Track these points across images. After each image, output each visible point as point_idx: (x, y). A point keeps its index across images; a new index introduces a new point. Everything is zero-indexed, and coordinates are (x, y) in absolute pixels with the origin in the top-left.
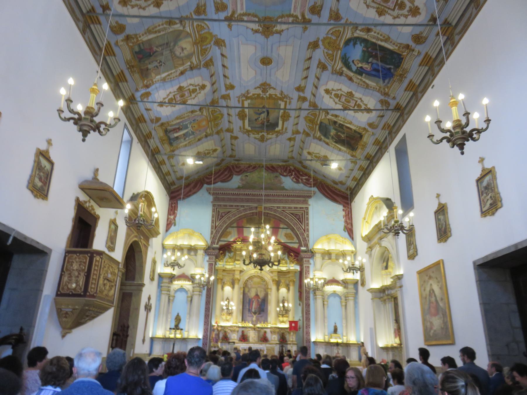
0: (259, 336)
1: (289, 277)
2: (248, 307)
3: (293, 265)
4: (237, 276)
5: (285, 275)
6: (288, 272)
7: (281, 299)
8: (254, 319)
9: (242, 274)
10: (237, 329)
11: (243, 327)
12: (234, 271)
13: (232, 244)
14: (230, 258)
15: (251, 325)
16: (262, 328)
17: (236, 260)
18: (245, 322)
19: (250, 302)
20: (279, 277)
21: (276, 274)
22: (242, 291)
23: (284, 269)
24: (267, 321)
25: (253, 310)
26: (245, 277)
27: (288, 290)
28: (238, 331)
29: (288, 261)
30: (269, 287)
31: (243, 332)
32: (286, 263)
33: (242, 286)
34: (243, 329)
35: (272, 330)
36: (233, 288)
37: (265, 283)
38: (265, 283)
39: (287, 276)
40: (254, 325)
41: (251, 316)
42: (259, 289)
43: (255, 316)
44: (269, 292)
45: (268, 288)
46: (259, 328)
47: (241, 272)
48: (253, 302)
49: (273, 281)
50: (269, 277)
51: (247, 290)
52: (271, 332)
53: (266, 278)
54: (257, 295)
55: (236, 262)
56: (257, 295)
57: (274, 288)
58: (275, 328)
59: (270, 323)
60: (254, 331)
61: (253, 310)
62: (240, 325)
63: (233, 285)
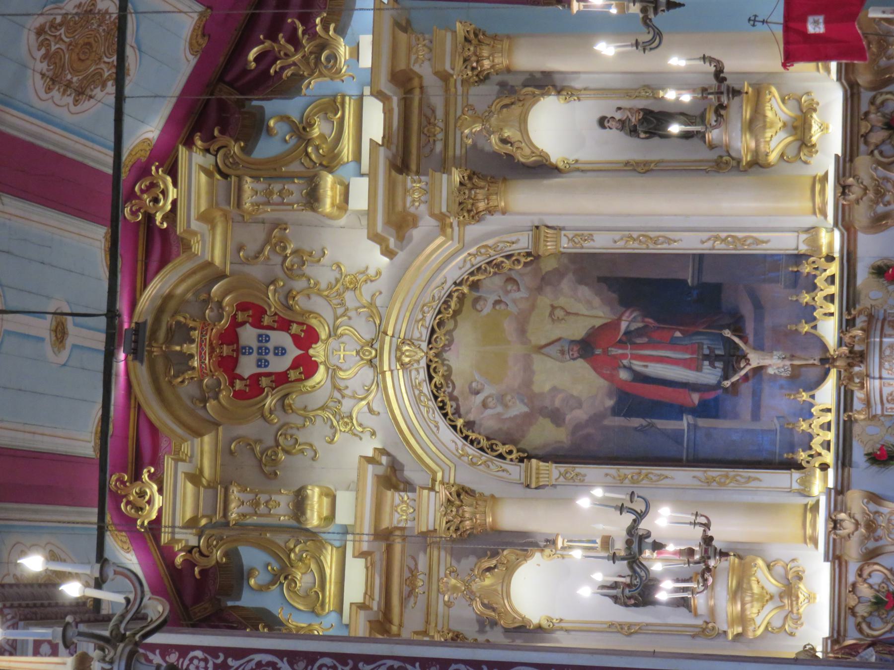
1: (445, 77)
2: (686, 422)
3: (343, 51)
4: (428, 511)
5: (428, 120)
6: (402, 84)
7: (618, 147)
8: (775, 364)
9: (411, 473)
10: (855, 500)
11: (844, 460)
12: (384, 536)
13: (167, 554)
14: (282, 574)
15: (827, 394)
16: (850, 298)
17: (297, 527)
18: (807, 441)
19: (638, 400)
20: (444, 167)
21: (413, 184)
22: (554, 471)
23: (375, 124)
24: (798, 258)
25: (709, 375)
26: (435, 446)
27: (545, 83)
28: (874, 498)
29: (314, 86)
30: (524, 242)
32: (331, 106)
33: (515, 471)
34: (858, 454)
35: (861, 215)
36: (525, 543)
37: (492, 284)
38: (492, 284)
39: (437, 102)
40: (827, 361)
41: (757, 396)
42: (543, 330)
43: (755, 359)
44: (565, 244)
45: (533, 257)
46: (846, 324)
47: (393, 477)
48: (641, 378)
49: (469, 211)
50: (439, 247)
51: (544, 433)
52: (878, 222)
53: (453, 272)
54: (585, 348)
55: (313, 520)
56: (585, 348)
57: (527, 202)
58: (843, 189)
59: (812, 231)
60: (874, 359)
61: (709, 375)
62: (820, 485)
63: (504, 547)
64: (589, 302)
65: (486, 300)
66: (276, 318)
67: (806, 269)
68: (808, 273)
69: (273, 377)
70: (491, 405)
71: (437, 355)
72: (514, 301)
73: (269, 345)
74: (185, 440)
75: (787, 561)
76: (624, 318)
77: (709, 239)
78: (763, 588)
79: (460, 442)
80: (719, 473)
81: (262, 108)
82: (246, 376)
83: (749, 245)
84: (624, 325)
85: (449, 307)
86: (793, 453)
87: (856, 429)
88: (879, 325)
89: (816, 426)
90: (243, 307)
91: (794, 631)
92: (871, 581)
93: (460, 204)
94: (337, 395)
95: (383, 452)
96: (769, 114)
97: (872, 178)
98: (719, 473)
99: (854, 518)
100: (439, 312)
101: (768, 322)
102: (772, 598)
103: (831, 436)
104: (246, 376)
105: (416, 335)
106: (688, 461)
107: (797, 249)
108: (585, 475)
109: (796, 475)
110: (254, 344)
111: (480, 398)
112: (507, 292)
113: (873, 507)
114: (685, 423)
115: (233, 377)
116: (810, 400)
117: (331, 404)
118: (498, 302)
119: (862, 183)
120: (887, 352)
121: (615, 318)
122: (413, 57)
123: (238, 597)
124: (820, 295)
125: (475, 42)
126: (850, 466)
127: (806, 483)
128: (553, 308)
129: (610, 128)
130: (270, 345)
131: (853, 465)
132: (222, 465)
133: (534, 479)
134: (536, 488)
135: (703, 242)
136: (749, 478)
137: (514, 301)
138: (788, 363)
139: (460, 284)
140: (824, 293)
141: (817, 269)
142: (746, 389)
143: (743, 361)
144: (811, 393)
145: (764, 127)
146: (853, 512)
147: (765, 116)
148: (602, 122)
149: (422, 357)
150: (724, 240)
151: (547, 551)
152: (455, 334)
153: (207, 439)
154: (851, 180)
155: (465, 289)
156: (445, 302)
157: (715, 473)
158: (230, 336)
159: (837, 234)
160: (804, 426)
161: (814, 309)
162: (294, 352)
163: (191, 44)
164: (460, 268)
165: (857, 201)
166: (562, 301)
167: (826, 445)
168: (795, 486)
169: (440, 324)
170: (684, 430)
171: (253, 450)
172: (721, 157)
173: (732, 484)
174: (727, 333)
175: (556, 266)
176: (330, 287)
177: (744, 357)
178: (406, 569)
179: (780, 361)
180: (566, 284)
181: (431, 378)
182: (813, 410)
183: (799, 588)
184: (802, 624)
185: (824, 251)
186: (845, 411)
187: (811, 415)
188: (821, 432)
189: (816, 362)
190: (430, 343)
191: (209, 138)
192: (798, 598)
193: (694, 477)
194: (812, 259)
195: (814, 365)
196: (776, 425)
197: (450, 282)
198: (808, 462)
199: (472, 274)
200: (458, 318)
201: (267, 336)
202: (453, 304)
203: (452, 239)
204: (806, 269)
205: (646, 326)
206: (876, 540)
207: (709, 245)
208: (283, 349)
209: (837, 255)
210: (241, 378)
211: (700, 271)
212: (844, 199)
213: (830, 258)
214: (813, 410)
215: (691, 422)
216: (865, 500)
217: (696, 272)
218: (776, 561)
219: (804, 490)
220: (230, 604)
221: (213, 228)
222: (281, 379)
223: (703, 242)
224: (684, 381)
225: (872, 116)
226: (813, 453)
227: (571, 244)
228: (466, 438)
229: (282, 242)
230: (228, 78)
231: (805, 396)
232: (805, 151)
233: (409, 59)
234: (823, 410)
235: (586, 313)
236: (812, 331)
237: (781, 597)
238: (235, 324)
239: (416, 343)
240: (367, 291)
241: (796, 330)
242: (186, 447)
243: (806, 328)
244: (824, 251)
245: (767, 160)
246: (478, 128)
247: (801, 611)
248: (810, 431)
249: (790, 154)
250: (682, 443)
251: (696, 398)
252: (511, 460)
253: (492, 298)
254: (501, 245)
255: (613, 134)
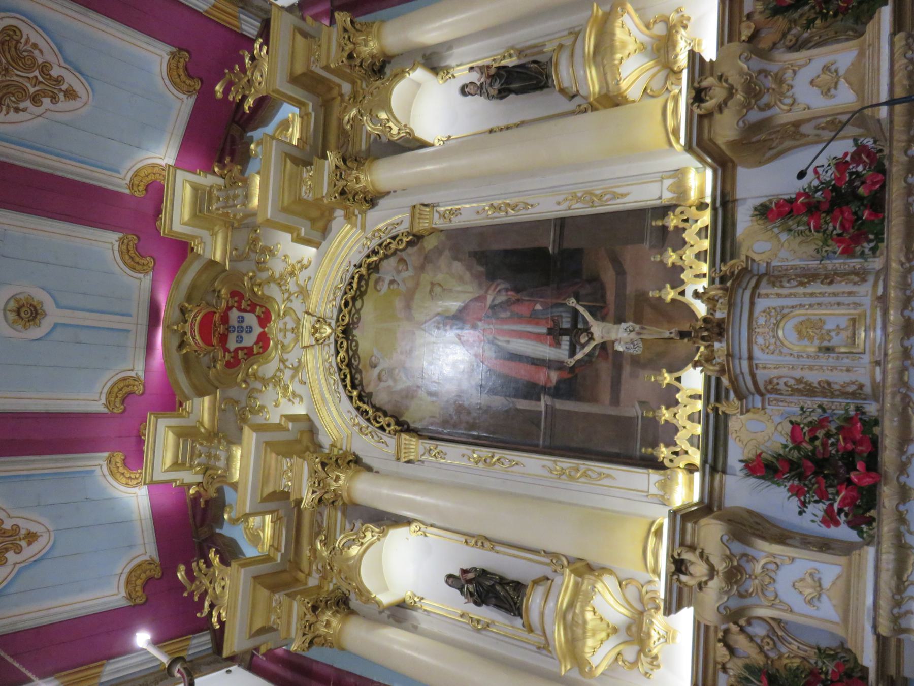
0: (807, 277)
11: (714, 465)
24: (664, 210)
31: (763, 468)
36: (386, 520)
45: (417, 239)
59: (679, 174)
62: (686, 491)
64: (461, 279)
65: (383, 281)
66: (249, 302)
67: (673, 221)
68: (676, 227)
69: (245, 351)
70: (384, 378)
71: (344, 332)
72: (404, 281)
73: (244, 325)
74: (188, 399)
75: (643, 583)
76: (490, 292)
77: (566, 200)
78: (601, 619)
79: (355, 412)
80: (569, 465)
81: (252, 137)
82: (232, 349)
83: (607, 201)
84: (490, 298)
85: (352, 287)
86: (655, 445)
87: (734, 424)
88: (753, 283)
89: (682, 417)
90: (233, 294)
91: (650, 672)
92: (750, 629)
93: (335, 185)
94: (282, 366)
95: (307, 418)
96: (620, 34)
97: (741, 73)
98: (569, 465)
99: (707, 561)
100: (346, 293)
101: (630, 289)
102: (615, 630)
103: (698, 430)
104: (232, 349)
105: (328, 314)
106: (544, 447)
107: (660, 198)
108: (446, 454)
109: (655, 476)
110: (236, 324)
111: (376, 372)
112: (399, 272)
113: (737, 548)
114: (542, 403)
115: (226, 350)
116: (676, 383)
117: (278, 374)
118: (392, 282)
119: (726, 81)
120: (762, 321)
121: (482, 292)
122: (312, 59)
123: (221, 528)
124: (689, 255)
125: (353, 31)
126: (724, 472)
127: (666, 486)
128: (432, 284)
129: (472, 95)
130: (244, 325)
131: (728, 470)
132: (219, 419)
133: (403, 455)
134: (409, 462)
135: (559, 204)
136: (600, 474)
137: (404, 281)
138: (633, 336)
139: (360, 266)
140: (696, 250)
141: (686, 220)
142: (605, 368)
143: (585, 334)
144: (677, 375)
145: (612, 50)
146: (706, 552)
147: (613, 34)
148: (464, 91)
149: (331, 334)
150: (579, 199)
151: (413, 527)
152: (362, 312)
153: (207, 400)
154: (709, 81)
155: (363, 270)
156: (350, 284)
157: (566, 464)
158: (225, 319)
159: (709, 173)
160: (665, 414)
161: (682, 270)
162: (258, 330)
163: (174, 83)
164: (360, 252)
165: (720, 108)
166: (440, 277)
167: (695, 440)
168: (654, 490)
169: (346, 304)
170: (541, 412)
171: (234, 408)
172: (580, 106)
173: (582, 480)
174: (572, 302)
175: (436, 244)
176: (281, 276)
177: (587, 330)
178: (316, 525)
179: (625, 335)
180: (443, 262)
181: (337, 352)
182: (678, 396)
183: (652, 622)
184: (658, 666)
185: (693, 196)
186: (718, 399)
187: (677, 403)
188: (689, 425)
189: (672, 336)
190: (337, 320)
191: (223, 166)
192: (649, 635)
193: (544, 467)
194: (679, 210)
195: (672, 339)
196: (635, 411)
197: (352, 264)
198: (671, 461)
199: (368, 256)
200: (365, 298)
201: (243, 317)
202: (355, 285)
203: (356, 226)
204: (673, 221)
205: (508, 301)
206: (741, 596)
207: (564, 206)
208: (251, 327)
209: (708, 200)
210: (229, 352)
211: (561, 236)
212: (698, 107)
213: (701, 206)
214: (678, 396)
215: (549, 403)
216: (725, 538)
217: (557, 238)
218: (630, 580)
219: (662, 497)
220: (218, 531)
221: (214, 235)
222: (249, 352)
223: (559, 204)
224: (542, 357)
225: (757, 17)
226: (678, 449)
227: (442, 221)
228: (358, 408)
229: (255, 242)
230: (236, 119)
231: (668, 378)
232: (673, 78)
233: (308, 60)
234: (691, 397)
235: (459, 288)
236: (680, 298)
237: (628, 628)
238: (229, 308)
239: (328, 320)
240: (302, 277)
241: (660, 297)
242: (188, 405)
243: (670, 294)
244: (693, 196)
245: (619, 89)
246: (354, 112)
247: (655, 651)
248: (674, 421)
249: (656, 85)
250: (538, 426)
251: (554, 376)
252: (390, 433)
253: (388, 278)
254: (390, 228)
255: (478, 102)
